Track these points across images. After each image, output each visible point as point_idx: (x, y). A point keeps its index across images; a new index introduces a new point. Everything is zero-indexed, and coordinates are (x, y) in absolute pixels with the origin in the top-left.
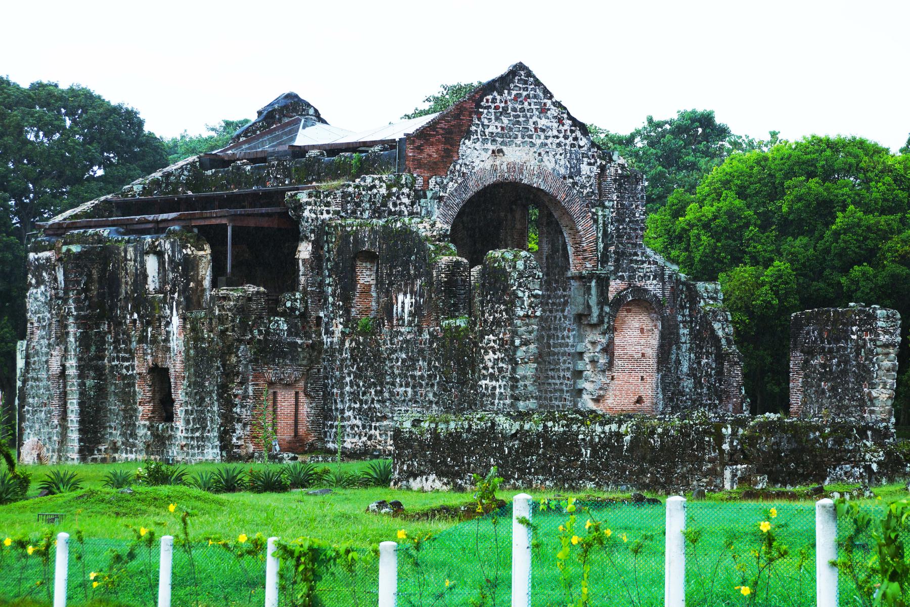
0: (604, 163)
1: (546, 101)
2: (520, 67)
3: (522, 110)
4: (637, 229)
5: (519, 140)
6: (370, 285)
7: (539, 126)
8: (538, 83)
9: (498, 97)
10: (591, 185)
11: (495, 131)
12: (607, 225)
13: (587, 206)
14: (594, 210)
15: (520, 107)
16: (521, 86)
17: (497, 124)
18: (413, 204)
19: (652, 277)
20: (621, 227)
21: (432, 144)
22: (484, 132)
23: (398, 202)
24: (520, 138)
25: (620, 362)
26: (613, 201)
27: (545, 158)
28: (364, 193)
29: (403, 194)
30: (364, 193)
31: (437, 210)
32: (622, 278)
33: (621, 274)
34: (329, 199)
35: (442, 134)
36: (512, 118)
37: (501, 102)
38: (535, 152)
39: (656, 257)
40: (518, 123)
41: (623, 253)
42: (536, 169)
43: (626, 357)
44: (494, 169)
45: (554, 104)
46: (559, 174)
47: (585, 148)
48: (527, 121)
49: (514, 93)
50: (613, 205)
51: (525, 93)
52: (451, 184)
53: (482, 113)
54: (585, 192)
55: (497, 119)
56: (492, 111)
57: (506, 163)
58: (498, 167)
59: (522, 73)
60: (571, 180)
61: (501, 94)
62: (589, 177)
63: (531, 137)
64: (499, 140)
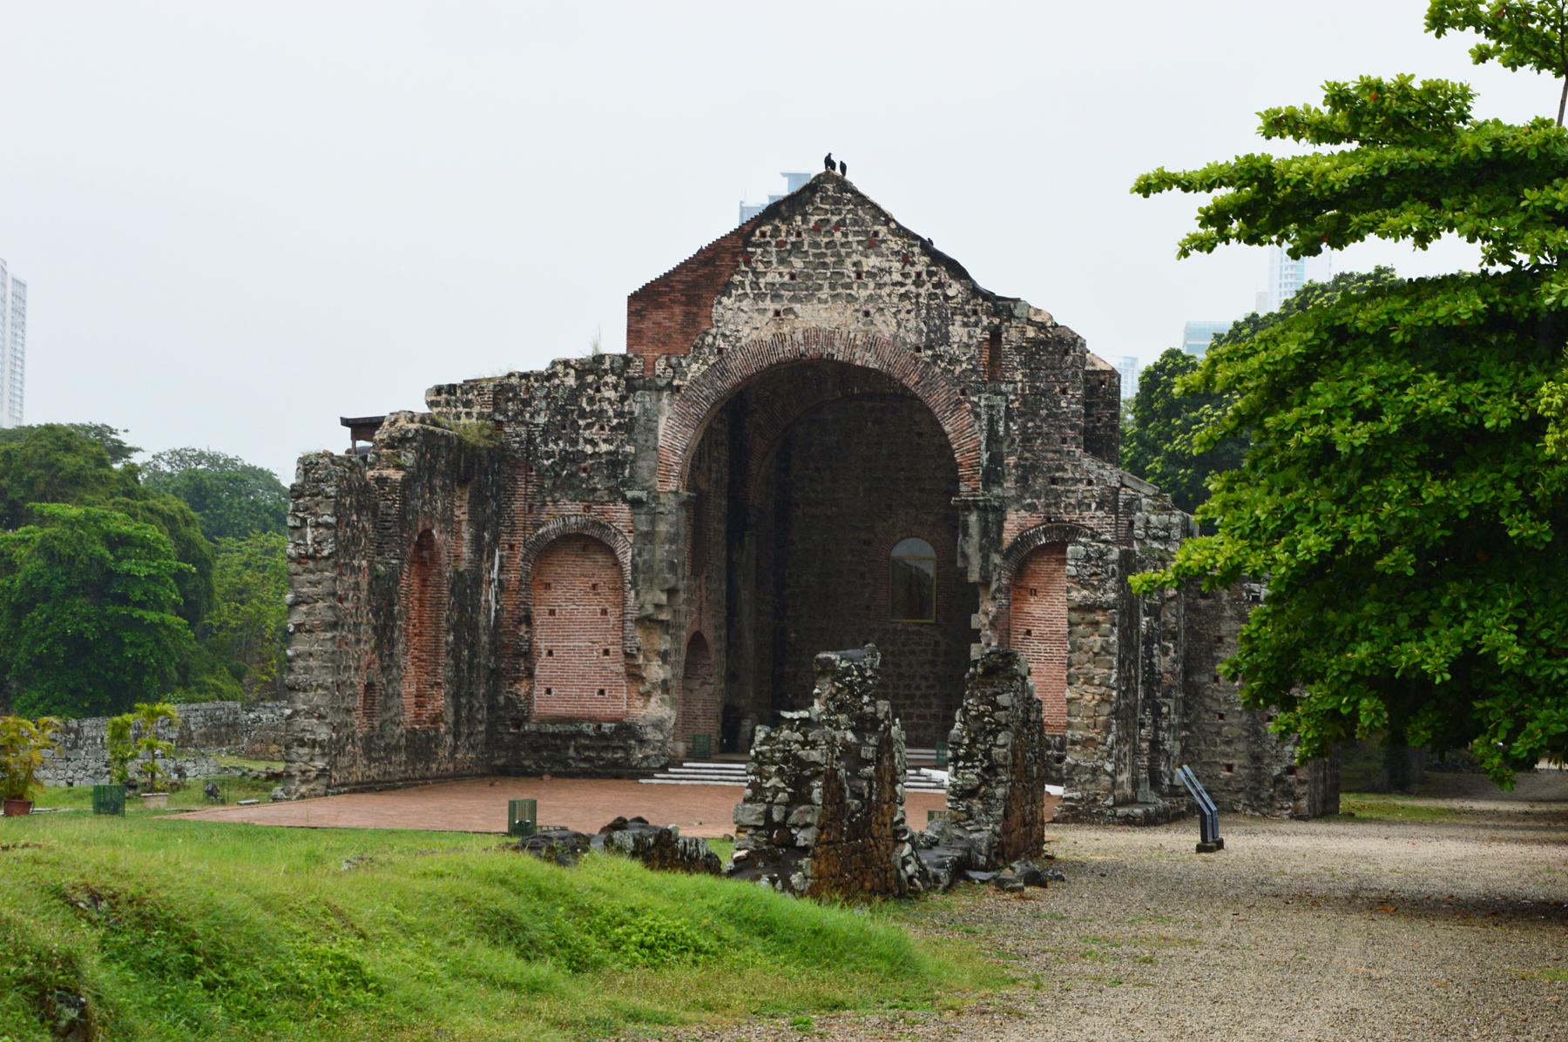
0: (996, 321)
1: (877, 228)
3: (830, 244)
4: (1061, 427)
5: (825, 293)
6: (459, 522)
7: (865, 269)
8: (861, 200)
9: (784, 228)
10: (972, 358)
11: (778, 279)
12: (997, 422)
13: (963, 393)
14: (976, 399)
15: (827, 240)
16: (827, 207)
17: (781, 269)
18: (623, 399)
19: (1094, 506)
21: (661, 306)
22: (757, 284)
23: (598, 396)
25: (1042, 647)
26: (1015, 383)
27: (878, 318)
28: (536, 385)
29: (606, 384)
30: (536, 385)
31: (667, 408)
32: (1032, 508)
33: (1029, 501)
34: (470, 396)
35: (679, 291)
36: (811, 258)
37: (788, 233)
38: (857, 310)
40: (825, 265)
42: (859, 337)
43: (1055, 637)
44: (780, 338)
45: (893, 233)
46: (905, 343)
48: (840, 262)
50: (1015, 389)
51: (835, 219)
52: (694, 366)
54: (958, 370)
55: (782, 262)
58: (788, 337)
59: (830, 186)
61: (787, 220)
62: (968, 346)
63: (848, 286)
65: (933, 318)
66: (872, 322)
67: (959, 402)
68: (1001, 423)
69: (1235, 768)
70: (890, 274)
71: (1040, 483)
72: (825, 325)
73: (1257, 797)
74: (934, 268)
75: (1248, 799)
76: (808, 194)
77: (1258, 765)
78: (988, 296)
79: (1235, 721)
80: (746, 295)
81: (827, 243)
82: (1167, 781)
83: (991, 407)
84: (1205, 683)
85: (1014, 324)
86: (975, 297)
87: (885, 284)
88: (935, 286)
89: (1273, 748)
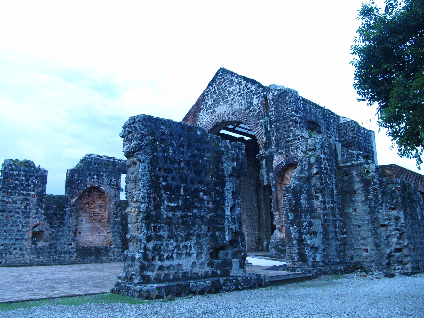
0: (265, 93)
1: (232, 78)
2: (222, 70)
8: (228, 72)
9: (211, 88)
10: (259, 108)
11: (211, 103)
12: (267, 126)
15: (221, 87)
16: (220, 78)
20: (278, 124)
24: (222, 101)
26: (272, 111)
27: (234, 105)
32: (281, 153)
33: (280, 151)
38: (229, 104)
39: (302, 134)
40: (221, 94)
41: (280, 139)
42: (230, 112)
44: (212, 120)
45: (236, 78)
46: (242, 110)
47: (255, 91)
49: (217, 82)
50: (273, 115)
51: (222, 80)
53: (205, 98)
54: (256, 113)
55: (212, 98)
56: (209, 95)
58: (214, 119)
59: (220, 72)
60: (248, 110)
62: (258, 104)
64: (213, 106)
65: (248, 99)
66: (233, 107)
67: (257, 124)
68: (269, 126)
69: (369, 251)
71: (282, 144)
72: (222, 112)
73: (380, 264)
75: (376, 265)
76: (216, 76)
77: (379, 248)
79: (365, 228)
80: (204, 110)
81: (221, 88)
82: (311, 259)
83: (265, 122)
84: (351, 212)
85: (270, 92)
86: (259, 88)
87: (235, 94)
88: (248, 89)
89: (385, 240)
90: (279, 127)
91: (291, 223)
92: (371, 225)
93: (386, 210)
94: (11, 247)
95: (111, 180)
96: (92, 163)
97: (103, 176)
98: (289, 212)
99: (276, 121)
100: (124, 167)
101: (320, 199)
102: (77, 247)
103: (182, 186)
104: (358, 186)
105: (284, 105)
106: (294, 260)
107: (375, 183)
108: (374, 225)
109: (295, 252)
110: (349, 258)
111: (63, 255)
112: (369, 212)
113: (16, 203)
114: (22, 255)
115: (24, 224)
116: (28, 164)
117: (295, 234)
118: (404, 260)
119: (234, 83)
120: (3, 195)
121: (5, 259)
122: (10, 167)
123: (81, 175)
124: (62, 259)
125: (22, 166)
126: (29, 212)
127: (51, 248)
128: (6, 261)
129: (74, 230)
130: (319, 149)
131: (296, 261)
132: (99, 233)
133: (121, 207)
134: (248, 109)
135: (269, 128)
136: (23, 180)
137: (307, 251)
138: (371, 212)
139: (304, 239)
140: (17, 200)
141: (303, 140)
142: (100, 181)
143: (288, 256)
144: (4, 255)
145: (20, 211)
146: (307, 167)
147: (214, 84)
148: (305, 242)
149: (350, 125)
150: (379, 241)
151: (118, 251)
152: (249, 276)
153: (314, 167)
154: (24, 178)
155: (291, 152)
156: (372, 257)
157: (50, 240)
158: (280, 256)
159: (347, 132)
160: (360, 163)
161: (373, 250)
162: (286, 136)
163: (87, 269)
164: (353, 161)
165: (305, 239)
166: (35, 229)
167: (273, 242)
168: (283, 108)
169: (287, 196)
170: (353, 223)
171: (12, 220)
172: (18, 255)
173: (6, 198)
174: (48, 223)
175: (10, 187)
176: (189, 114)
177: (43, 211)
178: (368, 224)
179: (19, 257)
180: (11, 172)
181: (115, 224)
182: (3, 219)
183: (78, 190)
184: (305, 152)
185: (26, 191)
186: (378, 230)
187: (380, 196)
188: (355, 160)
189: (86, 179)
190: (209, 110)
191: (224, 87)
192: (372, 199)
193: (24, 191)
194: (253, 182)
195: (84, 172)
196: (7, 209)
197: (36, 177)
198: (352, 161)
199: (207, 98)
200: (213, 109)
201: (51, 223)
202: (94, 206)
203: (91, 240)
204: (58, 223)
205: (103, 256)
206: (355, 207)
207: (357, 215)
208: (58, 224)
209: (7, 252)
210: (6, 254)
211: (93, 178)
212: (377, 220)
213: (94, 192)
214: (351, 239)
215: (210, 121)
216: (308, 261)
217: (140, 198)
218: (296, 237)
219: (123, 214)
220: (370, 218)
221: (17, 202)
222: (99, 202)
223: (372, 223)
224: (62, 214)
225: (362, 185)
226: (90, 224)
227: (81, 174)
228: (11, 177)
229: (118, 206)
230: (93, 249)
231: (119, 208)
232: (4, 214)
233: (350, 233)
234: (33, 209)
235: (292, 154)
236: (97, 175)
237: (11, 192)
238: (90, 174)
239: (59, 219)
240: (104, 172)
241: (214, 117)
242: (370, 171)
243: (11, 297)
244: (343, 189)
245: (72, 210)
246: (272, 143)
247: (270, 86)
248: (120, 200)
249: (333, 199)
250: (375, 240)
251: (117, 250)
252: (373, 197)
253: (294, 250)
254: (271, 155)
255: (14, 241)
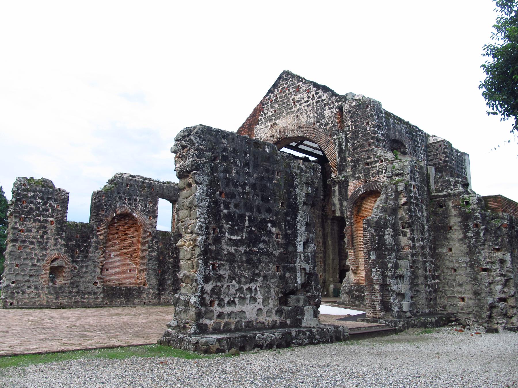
0: (340, 103)
1: (299, 84)
8: (293, 76)
10: (332, 122)
11: (271, 114)
12: (342, 144)
15: (284, 94)
16: (284, 83)
24: (285, 112)
26: (349, 126)
27: (301, 117)
32: (359, 178)
33: (357, 175)
38: (294, 116)
39: (386, 155)
40: (284, 103)
41: (358, 160)
42: (295, 126)
44: (272, 135)
45: (304, 83)
46: (310, 123)
47: (327, 100)
49: (280, 89)
51: (286, 86)
54: (328, 127)
55: (272, 107)
56: (269, 104)
57: (278, 129)
58: (275, 133)
59: (284, 76)
60: (318, 124)
61: (273, 93)
62: (331, 117)
64: (273, 118)
65: (318, 110)
67: (330, 141)
68: (344, 144)
69: (466, 300)
70: (304, 99)
71: (361, 167)
72: (285, 125)
73: (480, 317)
74: (318, 91)
75: (475, 318)
76: (278, 81)
77: (479, 297)
78: (336, 95)
79: (462, 272)
80: (263, 122)
81: (285, 95)
82: (396, 309)
83: (339, 139)
85: (347, 102)
86: (332, 97)
87: (302, 103)
88: (319, 98)
89: (486, 287)
90: (356, 145)
91: (373, 263)
92: (470, 269)
93: (489, 251)
94: (24, 285)
95: (146, 206)
96: (124, 184)
97: (136, 200)
98: (371, 250)
99: (352, 138)
100: (162, 190)
101: (409, 235)
102: (104, 286)
103: (247, 215)
104: (455, 221)
105: (363, 118)
106: (376, 308)
107: (476, 218)
108: (474, 269)
109: (377, 299)
110: (441, 309)
111: (86, 296)
112: (467, 252)
113: (31, 231)
114: (38, 295)
115: (40, 258)
116: (46, 184)
117: (377, 277)
118: (509, 313)
119: (301, 89)
120: (16, 220)
121: (17, 300)
122: (23, 187)
123: (110, 199)
124: (86, 300)
125: (38, 186)
126: (47, 242)
127: (72, 288)
128: (18, 302)
129: (101, 266)
130: (408, 174)
131: (378, 311)
132: (130, 270)
133: (158, 239)
134: (318, 122)
135: (344, 147)
136: (39, 203)
137: (392, 298)
138: (471, 252)
139: (388, 283)
140: (32, 227)
141: (387, 163)
142: (132, 206)
143: (369, 304)
144: (16, 294)
145: (35, 241)
146: (393, 196)
147: (276, 90)
148: (390, 287)
149: (442, 145)
150: (479, 288)
151: (154, 293)
152: (325, 327)
153: (401, 196)
154: (41, 201)
155: (371, 177)
156: (469, 307)
157: (72, 278)
158: (354, 303)
159: (437, 154)
160: (458, 192)
161: (472, 299)
162: (366, 157)
163: (119, 314)
164: (450, 189)
165: (390, 283)
166: (53, 263)
167: (346, 286)
168: (362, 123)
169: (369, 230)
170: (446, 265)
171: (26, 252)
172: (32, 295)
173: (18, 224)
174: (69, 256)
175: (23, 211)
176: (243, 126)
177: (63, 242)
178: (466, 268)
179: (33, 298)
180: (25, 193)
181: (150, 260)
182: (15, 250)
183: (105, 217)
184: (390, 177)
185: (43, 217)
186: (478, 276)
187: (482, 234)
188: (452, 189)
189: (115, 203)
190: (269, 123)
191: (289, 94)
192: (472, 237)
193: (40, 216)
194: (318, 212)
195: (113, 196)
196: (19, 239)
197: (56, 200)
198: (448, 189)
199: (267, 107)
200: (273, 121)
201: (72, 257)
202: (124, 237)
203: (121, 279)
204: (81, 256)
205: (135, 298)
206: (450, 247)
207: (452, 256)
208: (81, 258)
209: (20, 291)
210: (18, 293)
211: (124, 203)
212: (477, 263)
213: (125, 219)
214: (444, 285)
215: (269, 136)
216: (393, 311)
217: (196, 229)
218: (378, 281)
219: (160, 247)
220: (468, 260)
221: (32, 230)
222: (130, 233)
223: (472, 266)
224: (86, 246)
225: (460, 220)
226: (119, 259)
227: (110, 197)
228: (24, 199)
229: (154, 237)
230: (123, 290)
231: (155, 240)
232: (17, 244)
233: (443, 278)
234: (51, 239)
235: (373, 180)
236: (129, 200)
237: (25, 218)
238: (120, 198)
239: (82, 251)
240: (137, 196)
241: (274, 131)
242: (471, 202)
243: (37, 346)
244: (436, 223)
245: (99, 241)
246: (348, 165)
247: (347, 94)
248: (156, 231)
249: (424, 235)
250: (475, 287)
251: (152, 291)
252: (474, 235)
253: (376, 297)
254: (345, 180)
255: (28, 278)
